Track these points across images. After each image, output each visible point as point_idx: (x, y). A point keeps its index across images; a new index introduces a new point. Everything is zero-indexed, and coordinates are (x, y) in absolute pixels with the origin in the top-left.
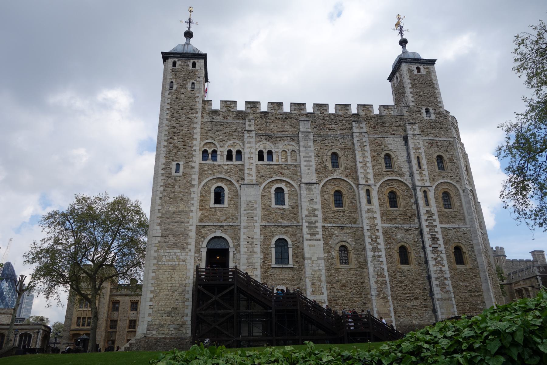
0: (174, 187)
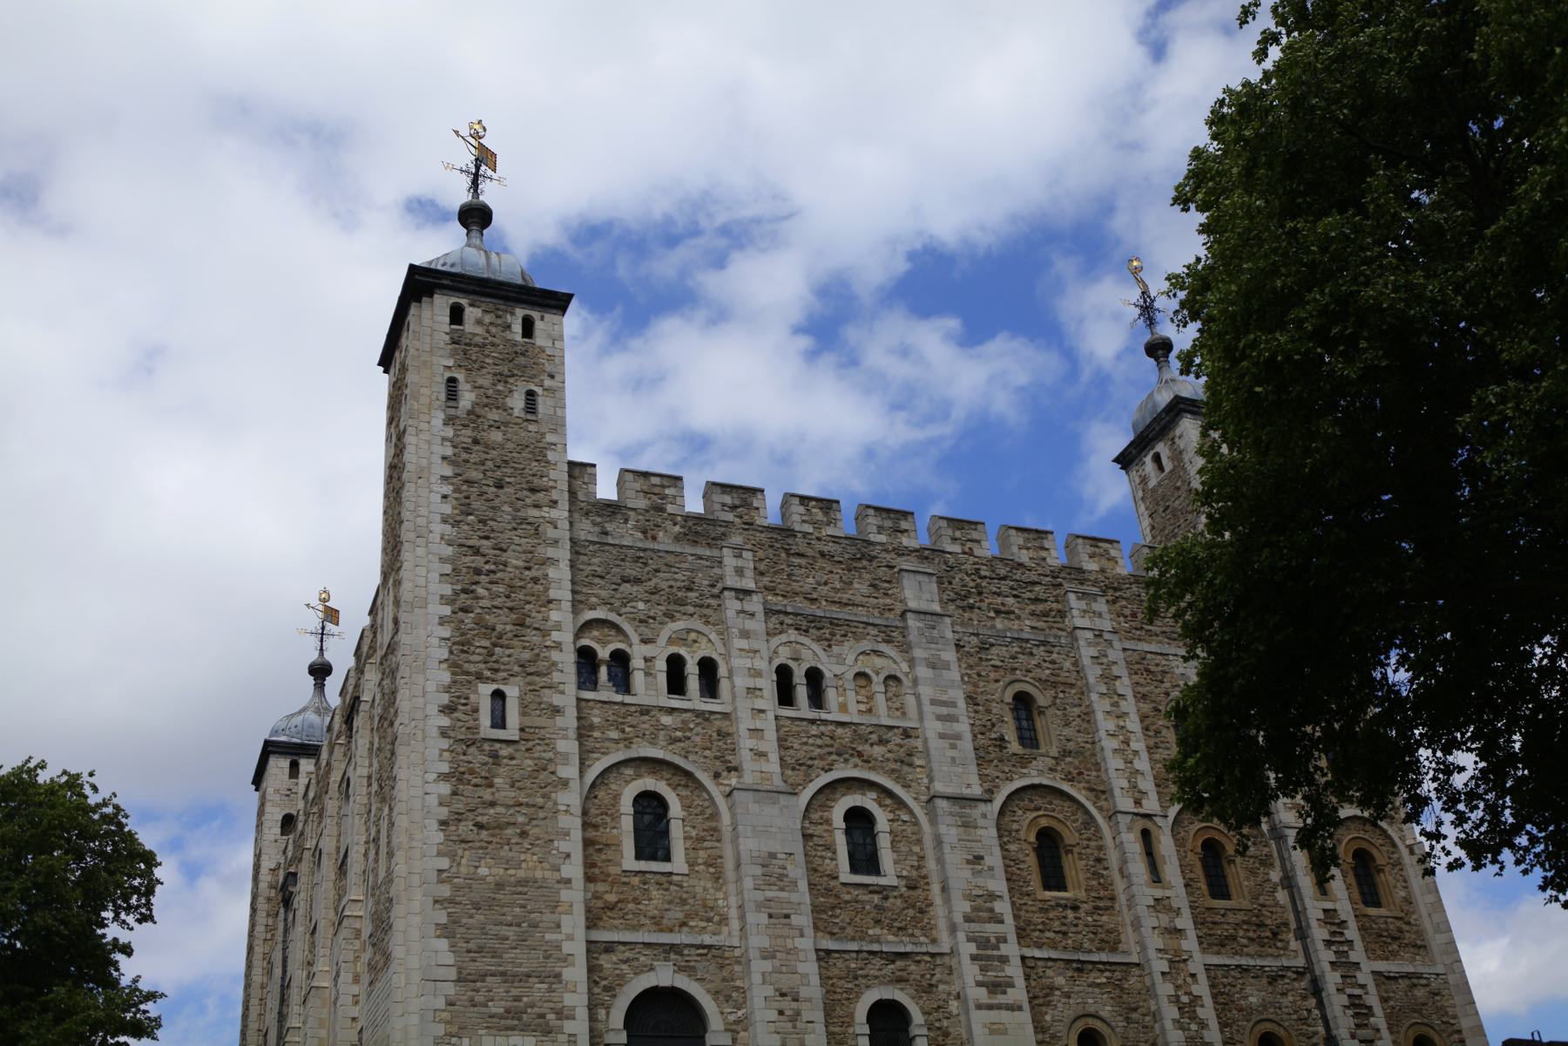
0: (491, 785)
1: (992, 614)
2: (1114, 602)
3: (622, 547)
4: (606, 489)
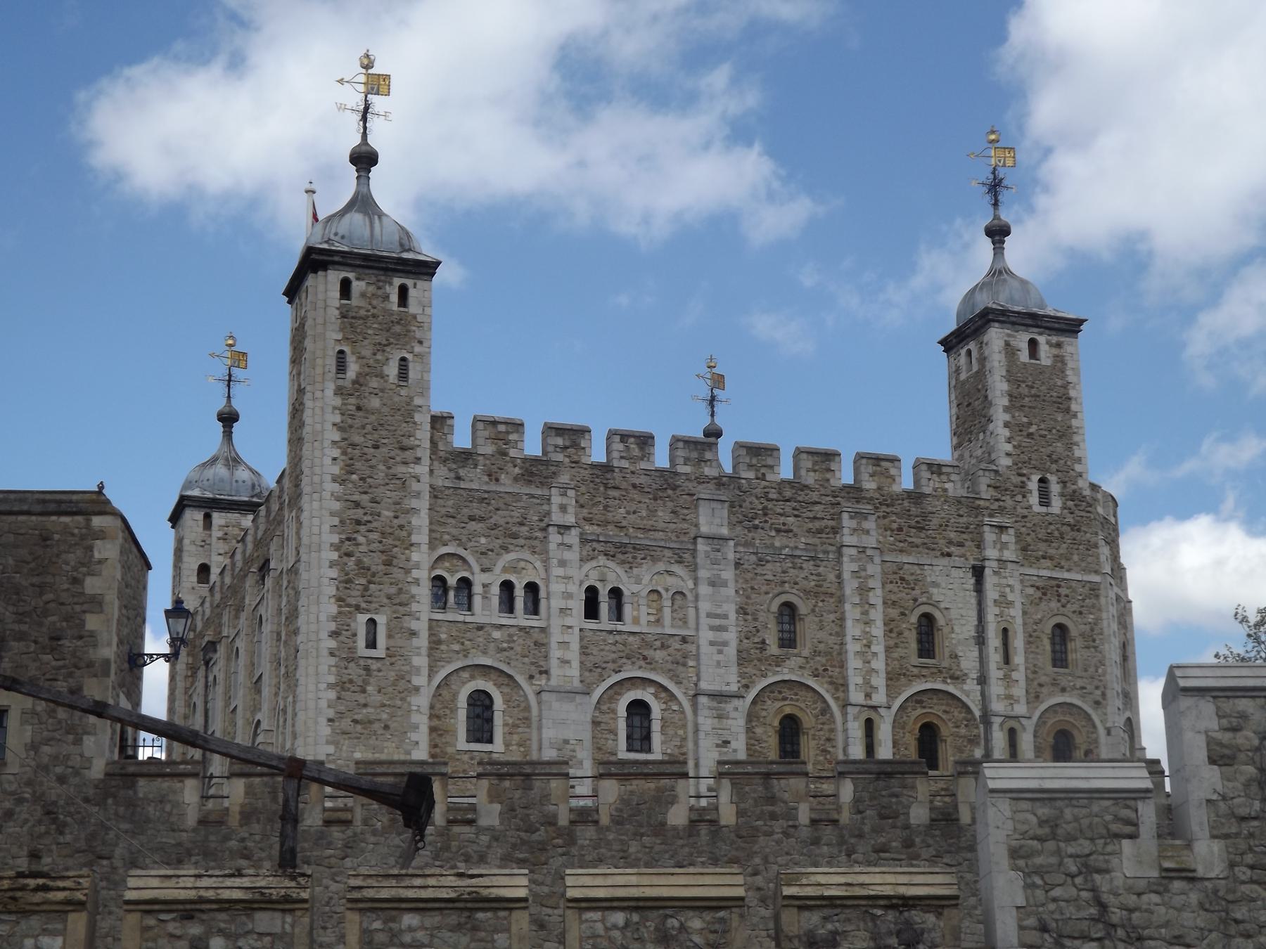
0: (364, 691)
1: (773, 533)
2: (884, 517)
3: (470, 490)
4: (461, 438)
